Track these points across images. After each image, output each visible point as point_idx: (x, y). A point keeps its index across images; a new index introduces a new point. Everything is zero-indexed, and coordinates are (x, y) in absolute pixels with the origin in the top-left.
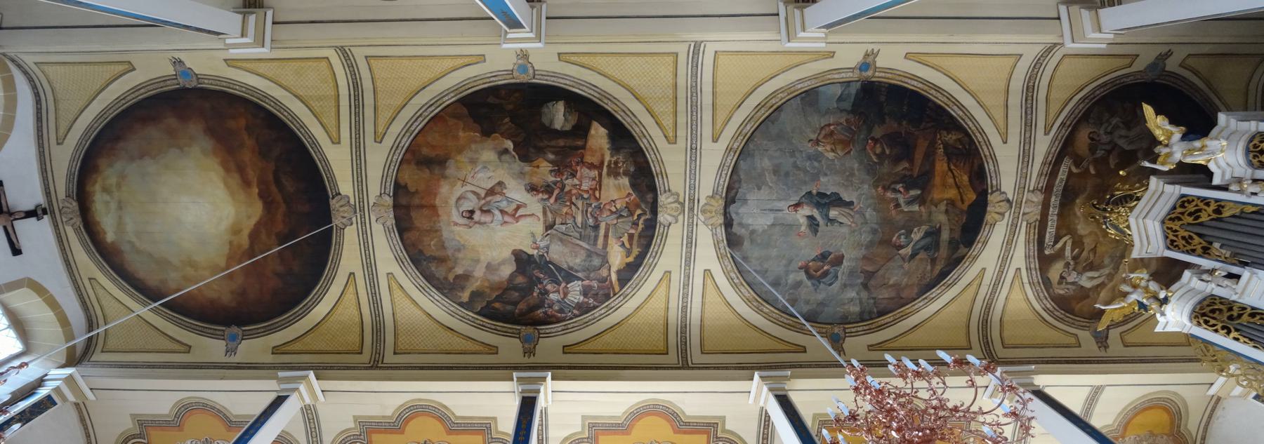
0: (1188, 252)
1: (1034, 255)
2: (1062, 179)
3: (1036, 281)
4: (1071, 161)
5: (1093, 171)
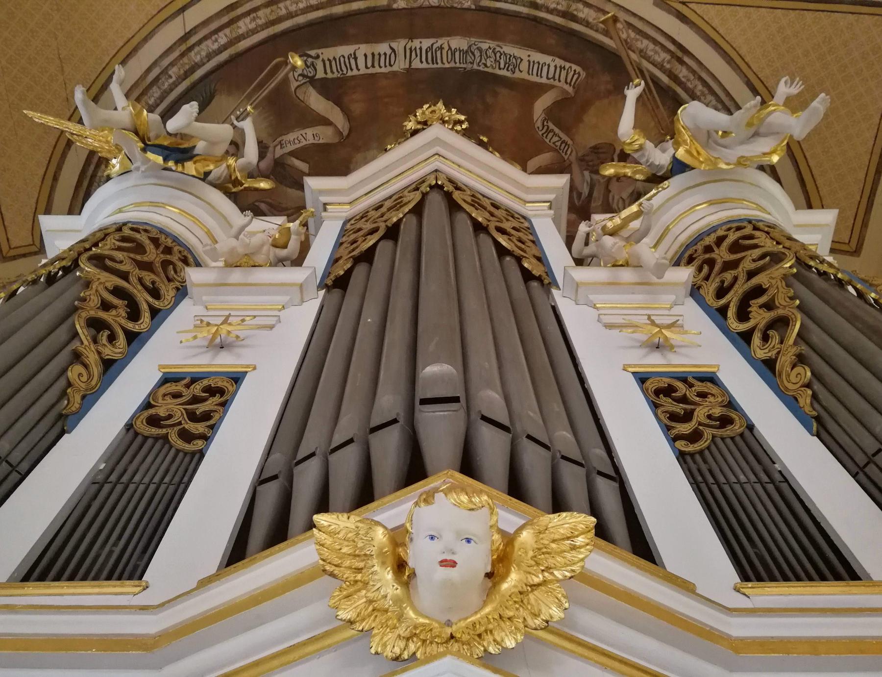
1: (279, 20)
2: (513, 63)
3: (195, 56)
4: (570, 89)
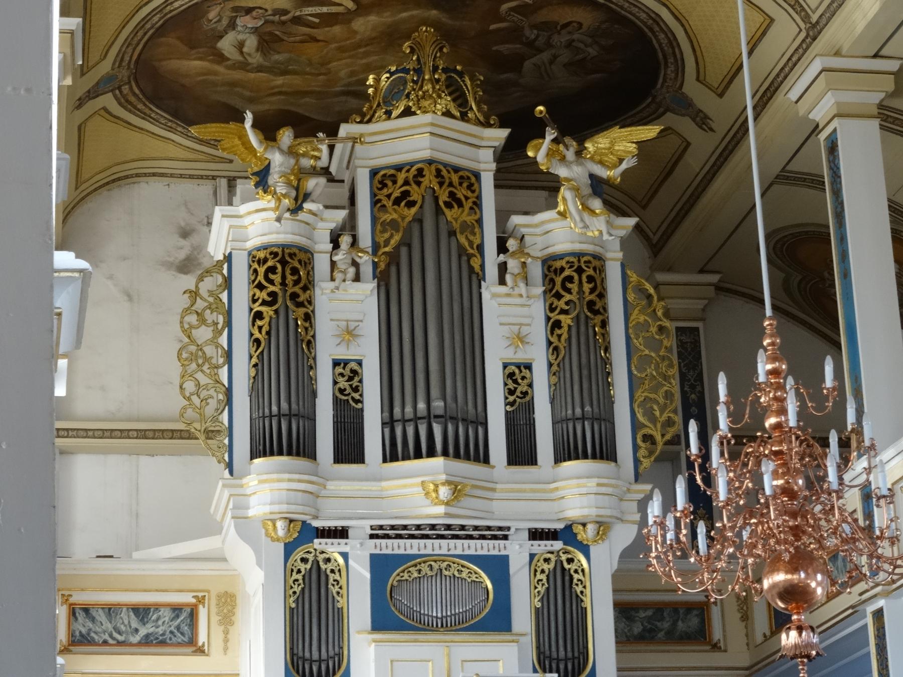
0: (375, 202)
5: (492, 27)
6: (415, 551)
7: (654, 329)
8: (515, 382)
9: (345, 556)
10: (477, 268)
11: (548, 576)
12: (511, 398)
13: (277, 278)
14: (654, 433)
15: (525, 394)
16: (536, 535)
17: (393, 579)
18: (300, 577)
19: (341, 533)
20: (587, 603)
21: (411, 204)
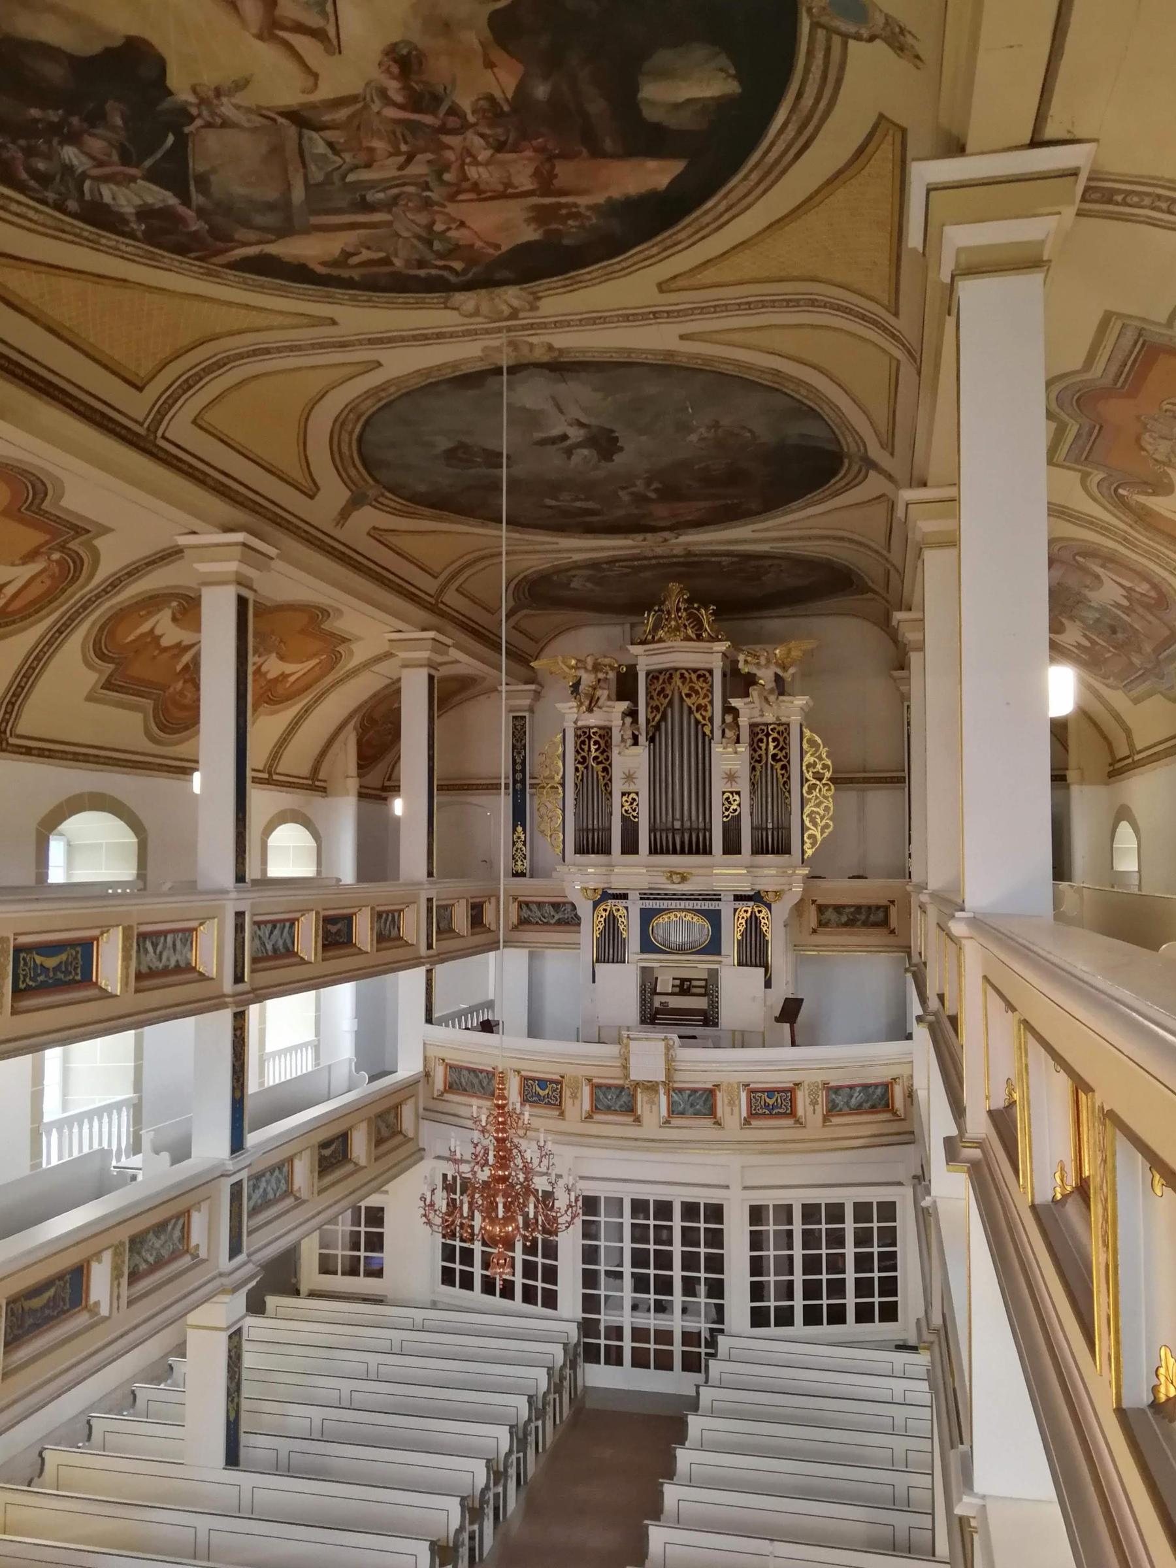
6: (665, 907)
7: (819, 766)
8: (730, 803)
9: (626, 908)
10: (708, 732)
11: (746, 921)
12: (727, 813)
13: (586, 748)
14: (816, 833)
15: (735, 810)
16: (738, 898)
17: (654, 922)
18: (602, 920)
19: (624, 897)
20: (769, 937)
21: (666, 697)
